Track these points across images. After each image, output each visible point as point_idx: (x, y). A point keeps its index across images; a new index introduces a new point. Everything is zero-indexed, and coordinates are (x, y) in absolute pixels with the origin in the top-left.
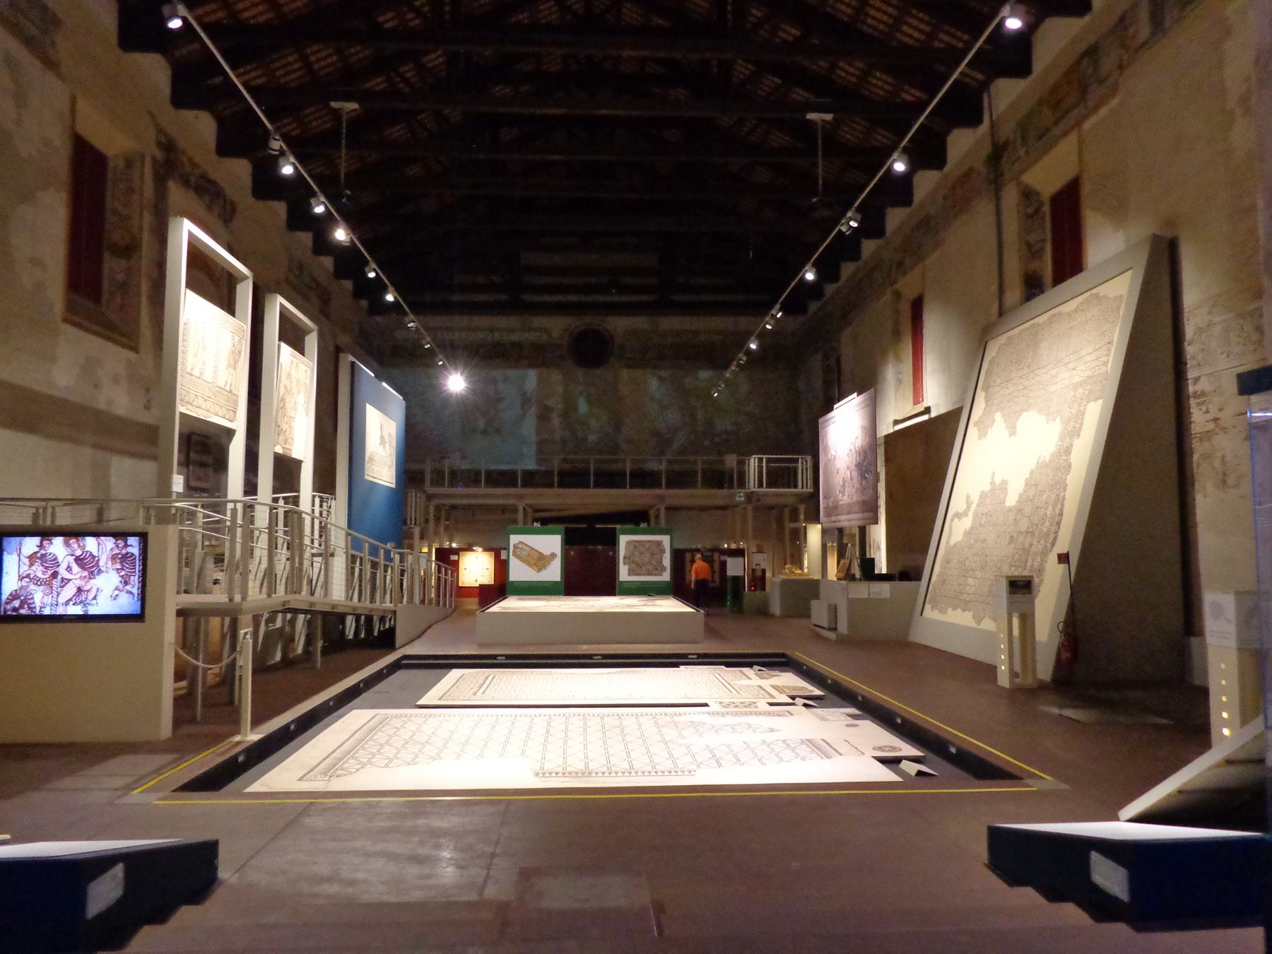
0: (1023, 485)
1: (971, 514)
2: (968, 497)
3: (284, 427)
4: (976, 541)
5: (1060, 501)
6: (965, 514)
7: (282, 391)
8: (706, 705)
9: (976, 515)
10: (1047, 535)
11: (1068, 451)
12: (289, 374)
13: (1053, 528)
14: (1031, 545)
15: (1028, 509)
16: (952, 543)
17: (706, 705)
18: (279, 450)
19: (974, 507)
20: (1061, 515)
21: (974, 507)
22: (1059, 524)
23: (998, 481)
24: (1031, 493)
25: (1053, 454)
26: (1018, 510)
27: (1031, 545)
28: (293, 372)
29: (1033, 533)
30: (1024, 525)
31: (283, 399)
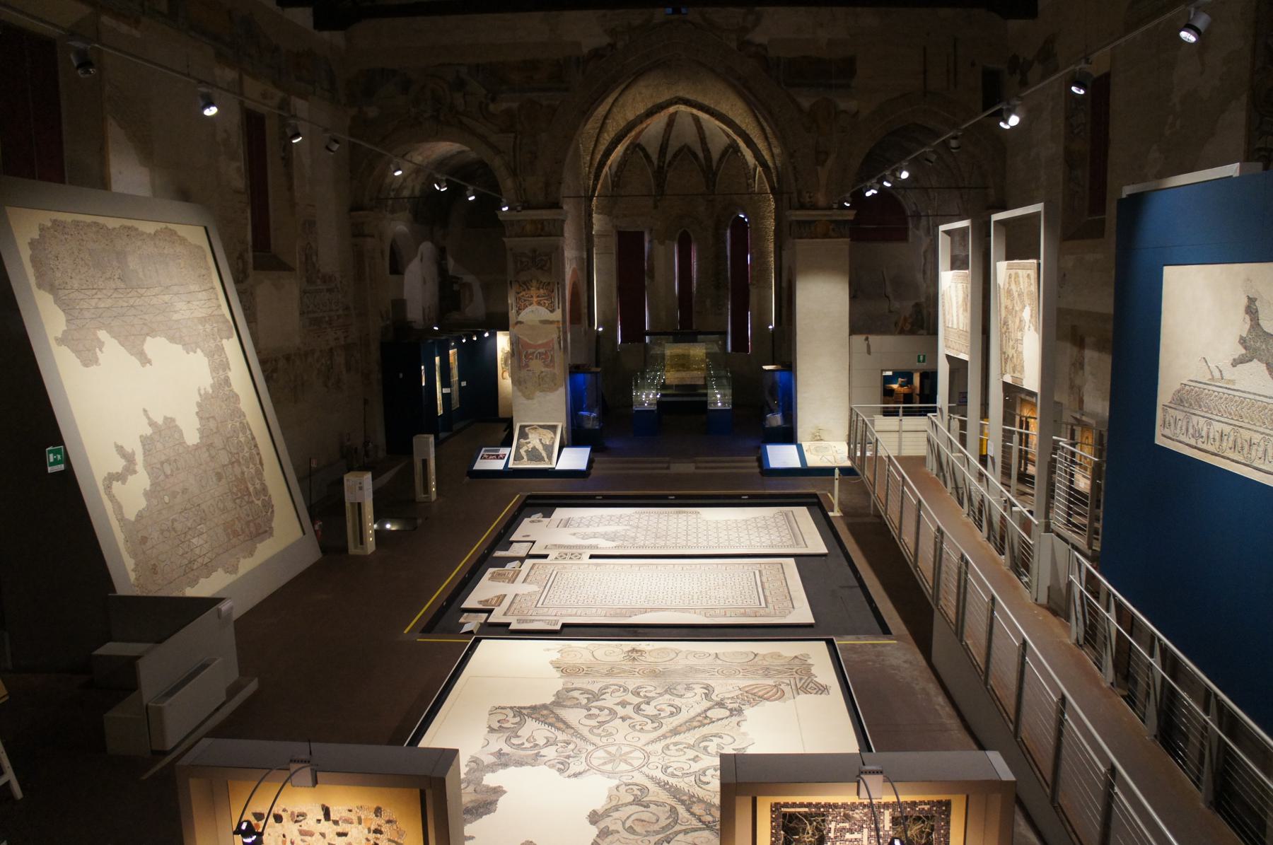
0: (197, 420)
1: (140, 466)
2: (120, 449)
3: (1011, 352)
4: (174, 495)
5: (245, 427)
6: (130, 469)
7: (1003, 315)
8: (592, 557)
9: (149, 466)
10: (252, 458)
11: (227, 381)
12: (1009, 292)
13: (254, 452)
14: (243, 473)
15: (218, 442)
16: (131, 515)
17: (592, 557)
18: (1008, 379)
19: (139, 458)
20: (253, 438)
21: (139, 458)
22: (256, 446)
23: (160, 421)
24: (212, 424)
25: (212, 386)
26: (207, 444)
27: (243, 473)
28: (1013, 287)
29: (238, 461)
30: (224, 458)
31: (1005, 323)
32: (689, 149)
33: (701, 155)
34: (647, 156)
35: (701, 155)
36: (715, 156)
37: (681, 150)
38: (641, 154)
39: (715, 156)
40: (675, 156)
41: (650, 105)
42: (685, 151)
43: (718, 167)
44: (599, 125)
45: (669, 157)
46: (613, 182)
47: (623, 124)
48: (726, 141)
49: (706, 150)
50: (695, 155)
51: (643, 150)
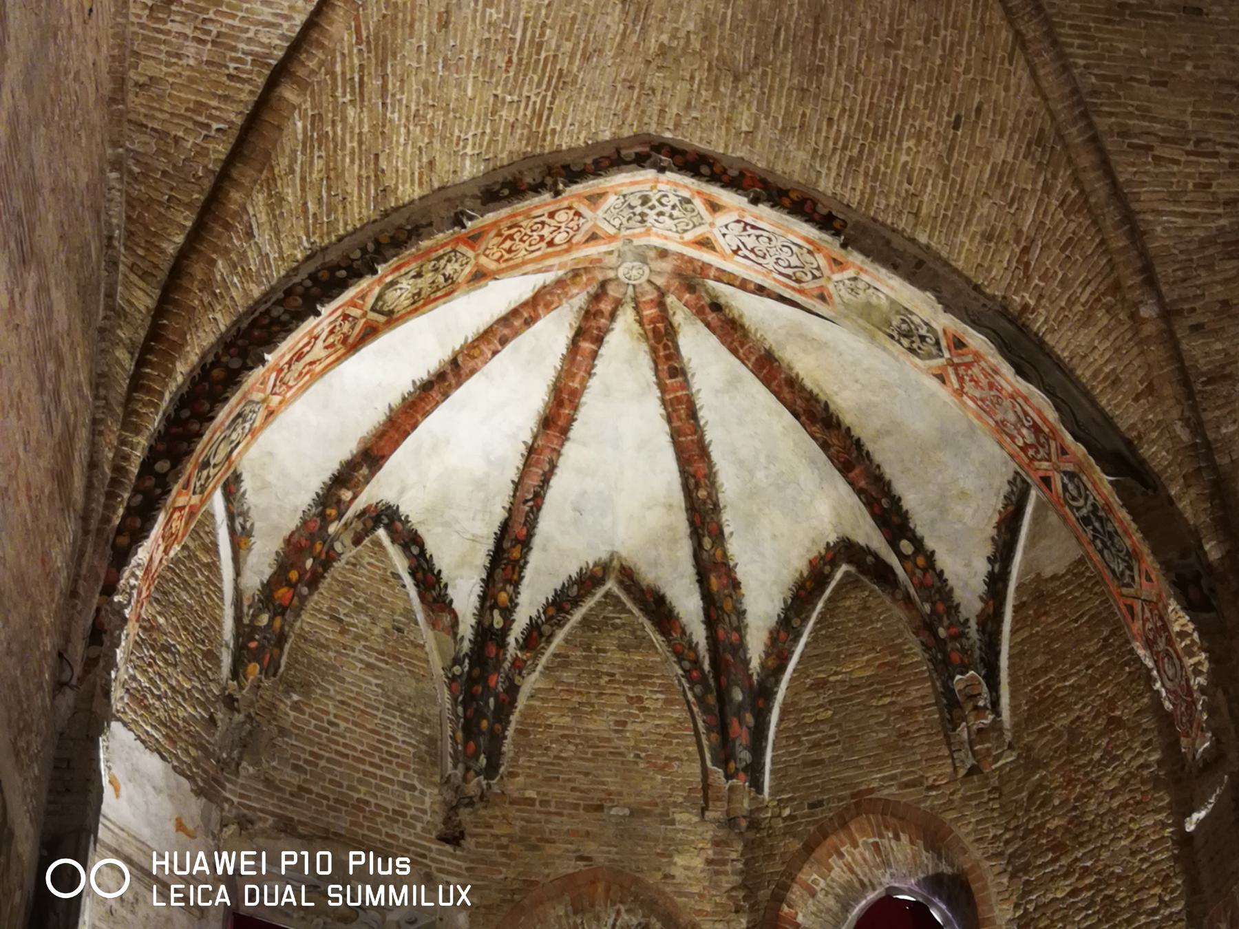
32: (628, 577)
33: (688, 604)
34: (427, 576)
35: (688, 604)
36: (761, 604)
37: (587, 581)
38: (399, 562)
39: (761, 604)
40: (561, 603)
41: (510, 147)
42: (612, 588)
43: (775, 668)
44: (234, 115)
45: (530, 600)
46: (244, 631)
47: (358, 210)
48: (824, 509)
49: (713, 569)
50: (657, 607)
51: (411, 542)
